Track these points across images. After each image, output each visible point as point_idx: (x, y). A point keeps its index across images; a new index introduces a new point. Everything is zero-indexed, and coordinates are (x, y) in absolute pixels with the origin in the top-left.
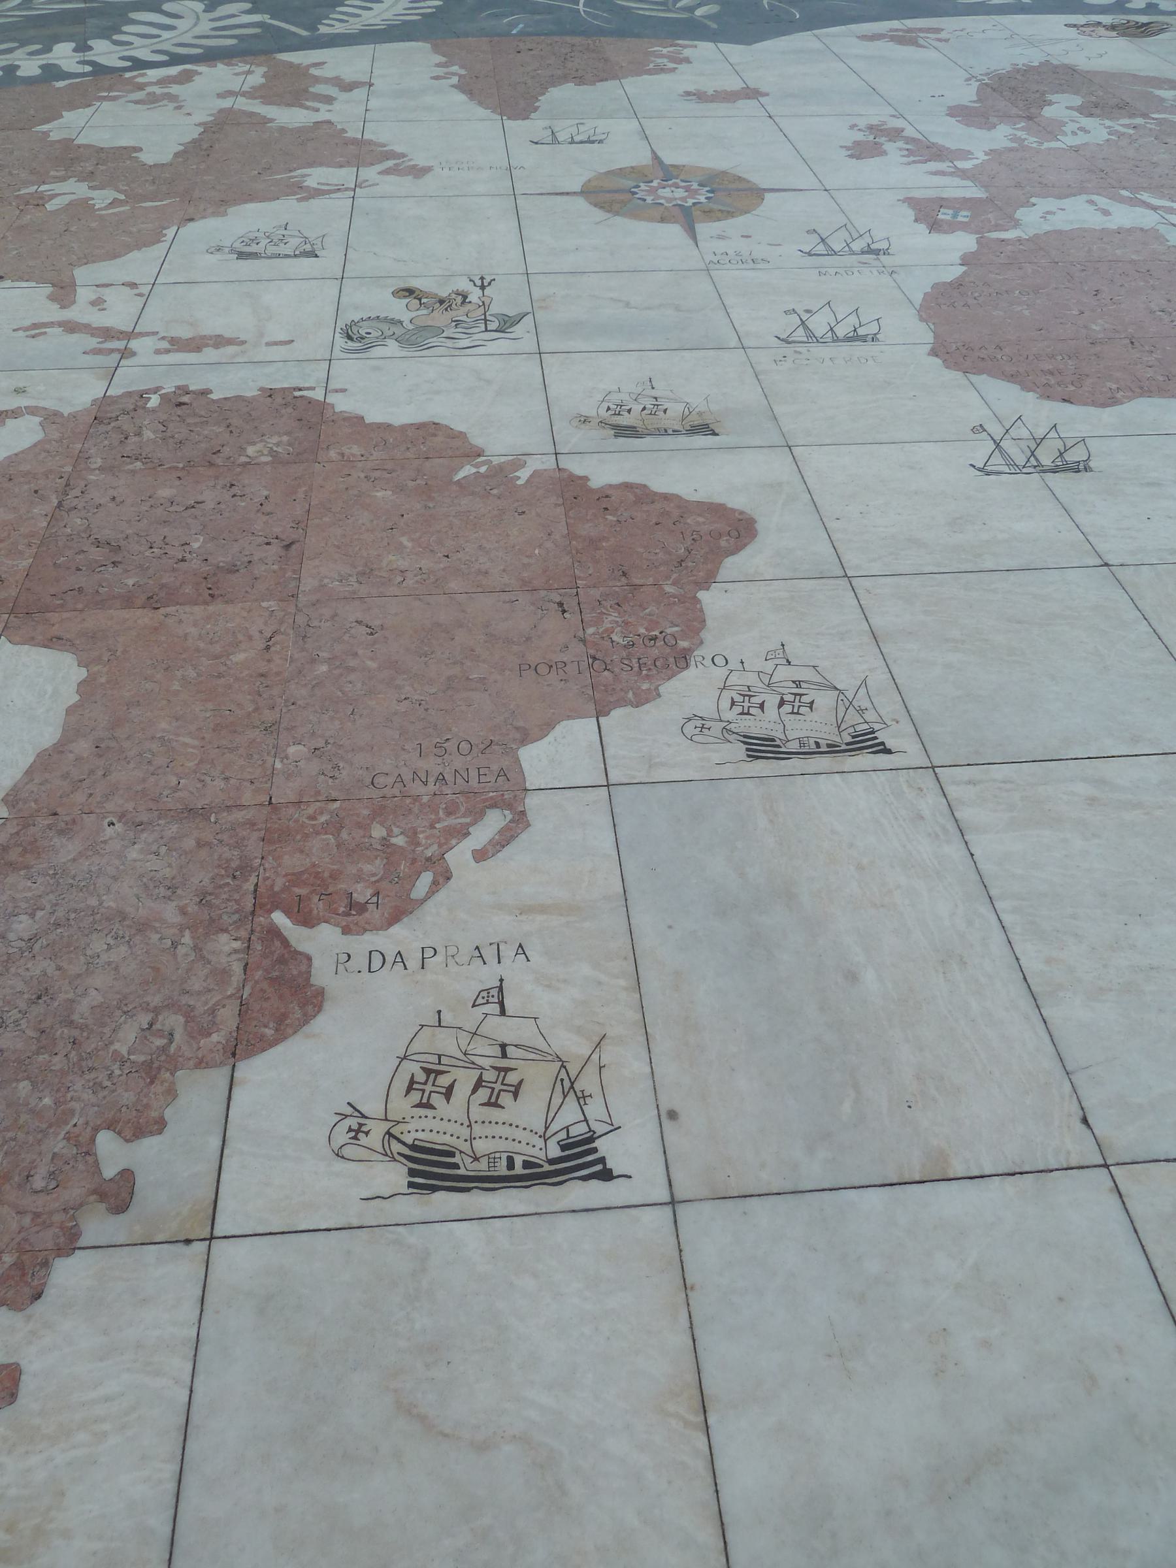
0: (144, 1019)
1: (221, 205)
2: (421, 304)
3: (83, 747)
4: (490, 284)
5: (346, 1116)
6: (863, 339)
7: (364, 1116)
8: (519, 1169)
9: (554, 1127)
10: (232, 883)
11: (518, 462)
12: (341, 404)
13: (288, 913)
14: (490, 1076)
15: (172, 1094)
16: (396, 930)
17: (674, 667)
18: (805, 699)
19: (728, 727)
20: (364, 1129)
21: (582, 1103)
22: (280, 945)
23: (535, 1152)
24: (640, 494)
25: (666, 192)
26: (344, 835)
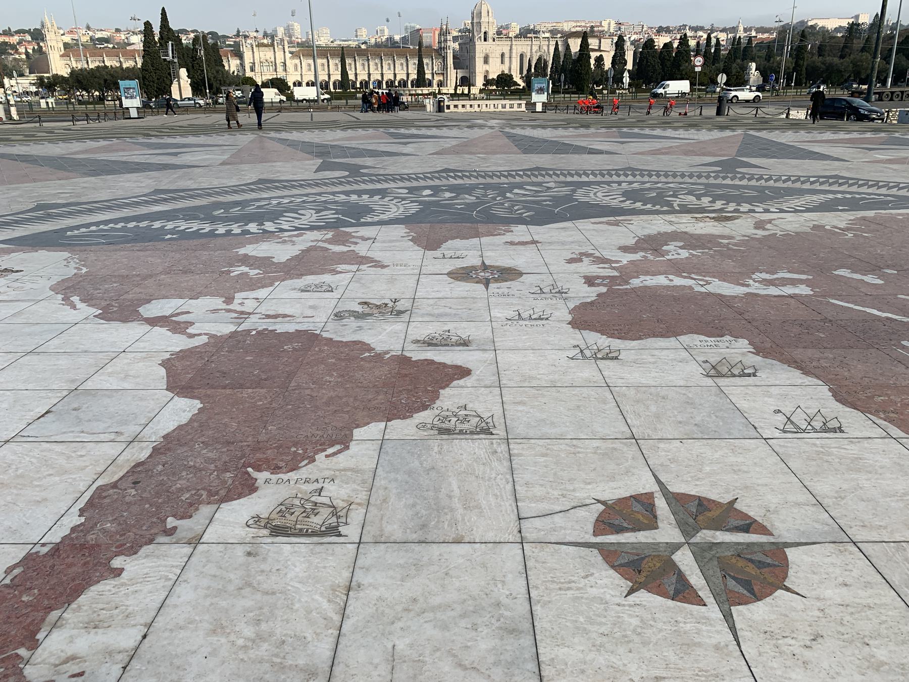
1: (300, 276)
3: (196, 424)
11: (387, 352)
15: (197, 509)
24: (432, 362)
25: (482, 274)
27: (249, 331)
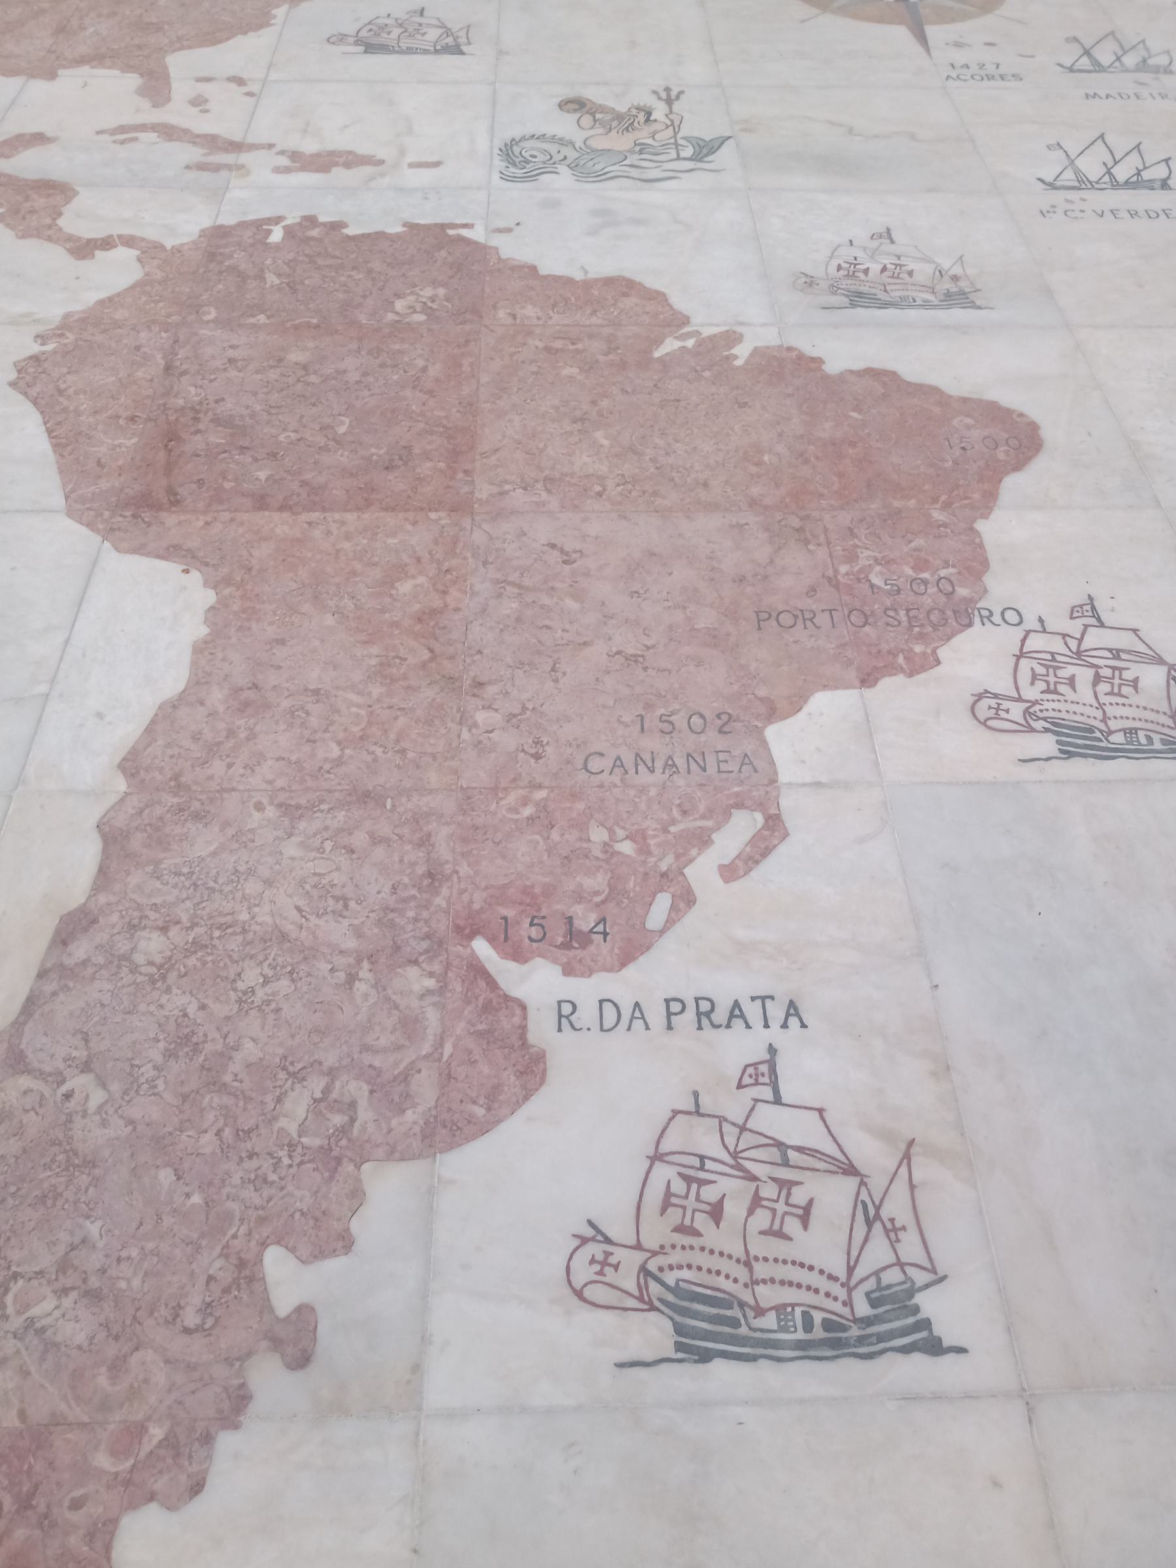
0: (316, 1085)
2: (595, 120)
3: (216, 696)
4: (678, 98)
5: (584, 1241)
6: (1149, 185)
7: (608, 1240)
8: (819, 1333)
9: (859, 1273)
10: (418, 896)
11: (732, 338)
12: (510, 249)
13: (492, 940)
14: (769, 1191)
15: (357, 1195)
16: (630, 971)
17: (954, 624)
18: (1127, 675)
19: (1031, 710)
20: (613, 1260)
21: (892, 1235)
22: (485, 986)
23: (837, 1307)
26: (555, 835)
27: (260, 226)
